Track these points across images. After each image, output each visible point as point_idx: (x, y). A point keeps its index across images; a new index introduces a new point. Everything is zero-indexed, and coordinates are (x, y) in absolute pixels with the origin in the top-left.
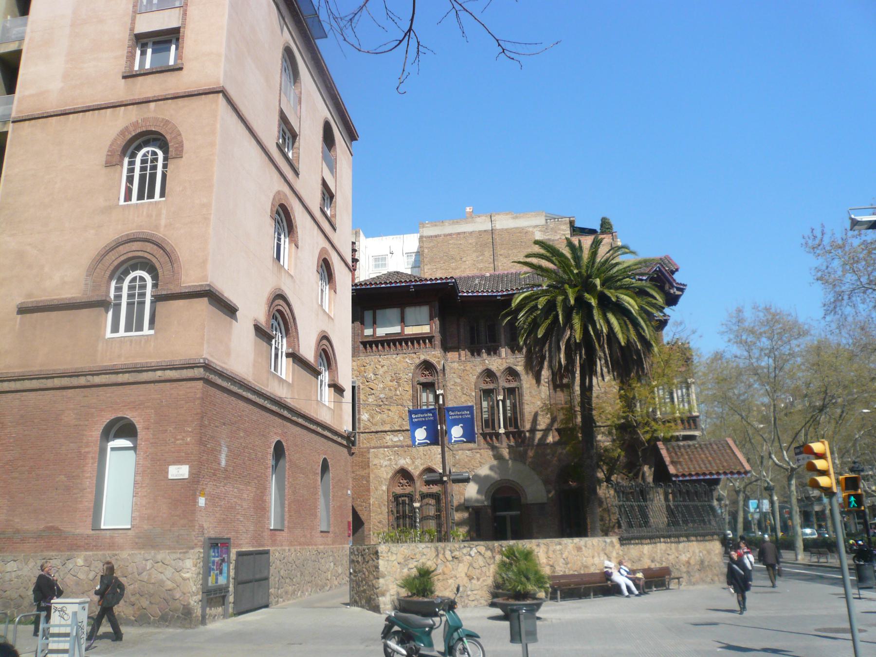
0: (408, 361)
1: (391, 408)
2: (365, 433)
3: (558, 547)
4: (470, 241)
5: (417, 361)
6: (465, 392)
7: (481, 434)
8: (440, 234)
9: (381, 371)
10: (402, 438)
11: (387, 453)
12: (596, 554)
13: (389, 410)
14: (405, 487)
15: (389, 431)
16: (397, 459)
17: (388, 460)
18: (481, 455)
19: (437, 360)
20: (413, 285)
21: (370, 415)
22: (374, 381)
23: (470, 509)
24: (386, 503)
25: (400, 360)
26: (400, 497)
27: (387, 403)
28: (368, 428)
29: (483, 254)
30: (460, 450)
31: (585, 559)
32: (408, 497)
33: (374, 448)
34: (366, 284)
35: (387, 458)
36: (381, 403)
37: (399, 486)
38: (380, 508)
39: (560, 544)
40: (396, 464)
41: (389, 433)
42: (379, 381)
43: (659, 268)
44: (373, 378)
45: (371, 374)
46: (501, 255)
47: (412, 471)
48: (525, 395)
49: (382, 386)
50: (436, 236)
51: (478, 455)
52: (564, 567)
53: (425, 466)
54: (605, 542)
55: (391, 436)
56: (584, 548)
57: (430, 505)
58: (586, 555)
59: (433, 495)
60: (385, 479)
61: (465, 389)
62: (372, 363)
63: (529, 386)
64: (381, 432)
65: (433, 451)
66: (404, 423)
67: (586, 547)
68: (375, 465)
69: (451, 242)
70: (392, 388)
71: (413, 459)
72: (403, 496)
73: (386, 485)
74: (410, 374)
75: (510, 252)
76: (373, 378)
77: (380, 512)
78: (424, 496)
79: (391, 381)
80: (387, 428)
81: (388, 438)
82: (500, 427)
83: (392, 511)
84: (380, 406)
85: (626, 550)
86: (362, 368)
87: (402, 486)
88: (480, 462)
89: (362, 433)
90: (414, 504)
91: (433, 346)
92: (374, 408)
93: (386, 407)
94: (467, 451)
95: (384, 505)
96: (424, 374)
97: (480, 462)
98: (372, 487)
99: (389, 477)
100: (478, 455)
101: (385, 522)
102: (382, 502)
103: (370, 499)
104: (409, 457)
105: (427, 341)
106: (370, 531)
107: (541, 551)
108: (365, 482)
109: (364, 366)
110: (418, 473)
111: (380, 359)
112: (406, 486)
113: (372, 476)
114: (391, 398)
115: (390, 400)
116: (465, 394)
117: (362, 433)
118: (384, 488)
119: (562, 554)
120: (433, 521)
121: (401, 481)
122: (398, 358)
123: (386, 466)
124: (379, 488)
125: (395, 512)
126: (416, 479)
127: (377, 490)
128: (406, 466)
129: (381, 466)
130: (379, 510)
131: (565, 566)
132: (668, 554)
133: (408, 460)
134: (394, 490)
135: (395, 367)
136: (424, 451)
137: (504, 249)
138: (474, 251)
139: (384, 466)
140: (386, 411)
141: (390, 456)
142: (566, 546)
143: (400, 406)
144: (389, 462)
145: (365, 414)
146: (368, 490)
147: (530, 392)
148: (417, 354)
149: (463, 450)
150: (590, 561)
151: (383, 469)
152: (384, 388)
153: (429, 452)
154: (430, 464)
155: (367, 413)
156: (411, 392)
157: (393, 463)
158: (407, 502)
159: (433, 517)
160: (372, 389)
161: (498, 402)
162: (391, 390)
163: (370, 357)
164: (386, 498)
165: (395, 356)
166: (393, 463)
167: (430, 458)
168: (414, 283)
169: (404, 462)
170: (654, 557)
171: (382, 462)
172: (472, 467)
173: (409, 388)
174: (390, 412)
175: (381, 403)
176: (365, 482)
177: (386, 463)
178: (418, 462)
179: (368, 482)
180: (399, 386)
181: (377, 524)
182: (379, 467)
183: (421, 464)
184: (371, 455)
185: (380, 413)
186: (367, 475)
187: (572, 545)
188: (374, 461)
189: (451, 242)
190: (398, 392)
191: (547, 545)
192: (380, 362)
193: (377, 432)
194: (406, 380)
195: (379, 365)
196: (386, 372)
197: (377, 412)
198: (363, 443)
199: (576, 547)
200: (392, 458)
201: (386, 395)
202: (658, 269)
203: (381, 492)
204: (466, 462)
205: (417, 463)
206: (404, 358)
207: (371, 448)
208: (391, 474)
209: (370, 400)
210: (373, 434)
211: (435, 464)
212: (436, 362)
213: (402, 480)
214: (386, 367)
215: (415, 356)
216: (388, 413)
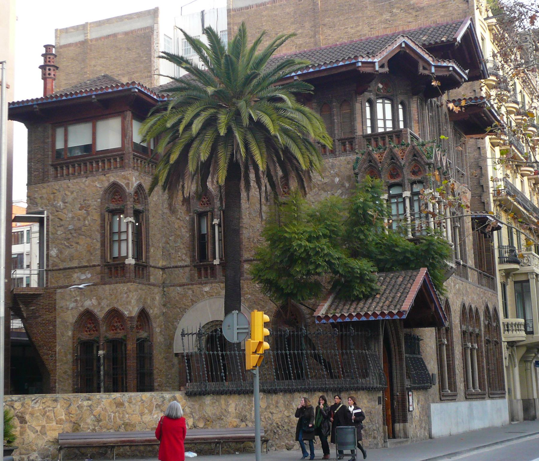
0: (98, 185)
1: (79, 241)
2: (53, 270)
3: (85, 403)
4: (287, 10)
5: (106, 184)
6: (178, 217)
7: (195, 266)
8: (251, 4)
9: (69, 199)
10: (89, 276)
11: (74, 293)
12: (146, 411)
13: (77, 243)
14: (92, 332)
15: (76, 268)
16: (83, 300)
17: (74, 302)
18: (193, 292)
19: (127, 181)
20: (95, 95)
21: (58, 250)
22: (64, 211)
23: (180, 357)
25: (89, 184)
27: (75, 235)
28: (56, 266)
29: (303, 27)
30: (171, 286)
31: (127, 416)
33: (61, 287)
34: (61, 96)
35: (73, 300)
36: (70, 236)
37: (87, 331)
38: (65, 357)
39: (89, 399)
40: (82, 306)
41: (76, 270)
42: (68, 210)
43: (406, 44)
44: (62, 207)
45: (61, 203)
46: (324, 25)
47: (98, 313)
48: (244, 217)
49: (70, 215)
50: (247, 8)
51: (190, 292)
52: (94, 425)
54: (163, 397)
55: (79, 274)
56: (126, 404)
58: (129, 411)
61: (179, 213)
62: (61, 189)
63: (248, 206)
64: (69, 268)
65: (119, 290)
66: (92, 258)
67: (130, 402)
68: (62, 307)
69: (264, 13)
70: (80, 217)
71: (99, 299)
74: (99, 200)
75: (336, 20)
76: (62, 207)
79: (80, 210)
80: (75, 264)
81: (75, 275)
82: (214, 258)
84: (69, 239)
85: (197, 407)
86: (52, 196)
88: (192, 301)
89: (50, 270)
91: (123, 167)
92: (63, 242)
93: (75, 239)
94: (178, 288)
96: (115, 199)
97: (192, 301)
98: (58, 333)
99: (74, 321)
100: (190, 292)
101: (70, 372)
103: (55, 346)
104: (95, 298)
105: (118, 160)
106: (55, 383)
107: (59, 406)
108: (51, 328)
109: (54, 193)
110: (103, 315)
111: (69, 185)
113: (58, 320)
114: (80, 229)
115: (79, 231)
116: (179, 219)
117: (50, 270)
118: (70, 333)
119: (91, 410)
122: (87, 182)
123: (72, 308)
126: (101, 322)
127: (63, 336)
129: (67, 309)
131: (96, 423)
132: (272, 413)
133: (94, 301)
134: (80, 336)
135: (84, 193)
136: (110, 290)
137: (329, 17)
138: (292, 23)
139: (70, 308)
140: (75, 245)
141: (77, 296)
142: (99, 402)
143: (88, 239)
144: (75, 304)
145: (54, 249)
146: (55, 336)
147: (250, 214)
148: (107, 175)
149: (173, 286)
150: (135, 419)
151: (69, 312)
152: (73, 218)
153: (115, 291)
154: (116, 306)
155: (55, 247)
156: (99, 222)
157: (79, 305)
160: (61, 220)
161: (213, 227)
162: (79, 220)
163: (60, 182)
164: (71, 346)
165: (84, 180)
166: (79, 305)
167: (116, 297)
168: (95, 93)
169: (89, 303)
170: (245, 416)
171: (68, 303)
172: (183, 306)
173: (96, 216)
174: (78, 246)
175: (70, 236)
176: (51, 328)
177: (72, 305)
178: (104, 303)
179: (55, 326)
180: (88, 214)
183: (107, 306)
184: (58, 296)
185: (68, 247)
186: (53, 319)
187: (109, 401)
188: (60, 303)
189: (264, 13)
190: (87, 222)
191: (69, 400)
192: (69, 187)
193: (65, 269)
194: (94, 207)
195: (69, 191)
196: (75, 198)
197: (66, 246)
198: (51, 282)
199: (115, 403)
200: (78, 298)
201: (74, 226)
202: (403, 45)
204: (177, 300)
205: (102, 304)
206: (93, 182)
207: (57, 288)
209: (59, 233)
210: (61, 271)
211: (121, 305)
212: (126, 184)
214: (75, 194)
215: (103, 178)
216: (77, 247)
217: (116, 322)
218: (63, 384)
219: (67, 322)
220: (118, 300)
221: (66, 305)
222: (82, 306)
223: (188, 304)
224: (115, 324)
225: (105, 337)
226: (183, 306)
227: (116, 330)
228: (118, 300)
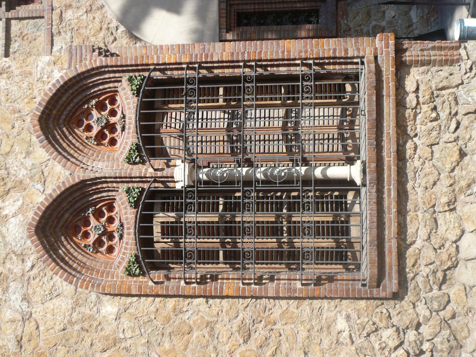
14: (117, 223)
18: (69, 6)
24: (171, 302)
26: (150, 242)
32: (149, 207)
37: (110, 250)
40: (22, 257)
51: (69, 15)
53: (34, 138)
57: (186, 124)
59: (150, 105)
60: (77, 304)
68: (19, 342)
72: (150, 231)
73: (99, 302)
77: (206, 332)
78: (148, 141)
83: (203, 280)
87: (111, 237)
90: (179, 186)
94: (55, 49)
95: (177, 311)
99: (68, 288)
102: (168, 319)
110: (58, 168)
112: (111, 220)
120: (251, 113)
121: (91, 240)
123: (26, 298)
124: (108, 330)
125: (209, 268)
126: (80, 175)
128: (31, 215)
130: (195, 334)
134: (121, 271)
144: (13, 285)
154: (28, 119)
158: (171, 216)
159: (233, 116)
166: (17, 270)
181: (252, 345)
182: (29, 327)
183: (28, 154)
203: (126, 323)
205: (22, 173)
208: (57, 278)
213: (86, 235)
217: (89, 128)
218: (285, 347)
219: (71, 323)
220: (14, 111)
221: (13, 321)
222: (22, 257)
223: (97, 20)
224: (96, 129)
225: (130, 160)
226: (101, 35)
227: (112, 128)
228: (14, 111)
